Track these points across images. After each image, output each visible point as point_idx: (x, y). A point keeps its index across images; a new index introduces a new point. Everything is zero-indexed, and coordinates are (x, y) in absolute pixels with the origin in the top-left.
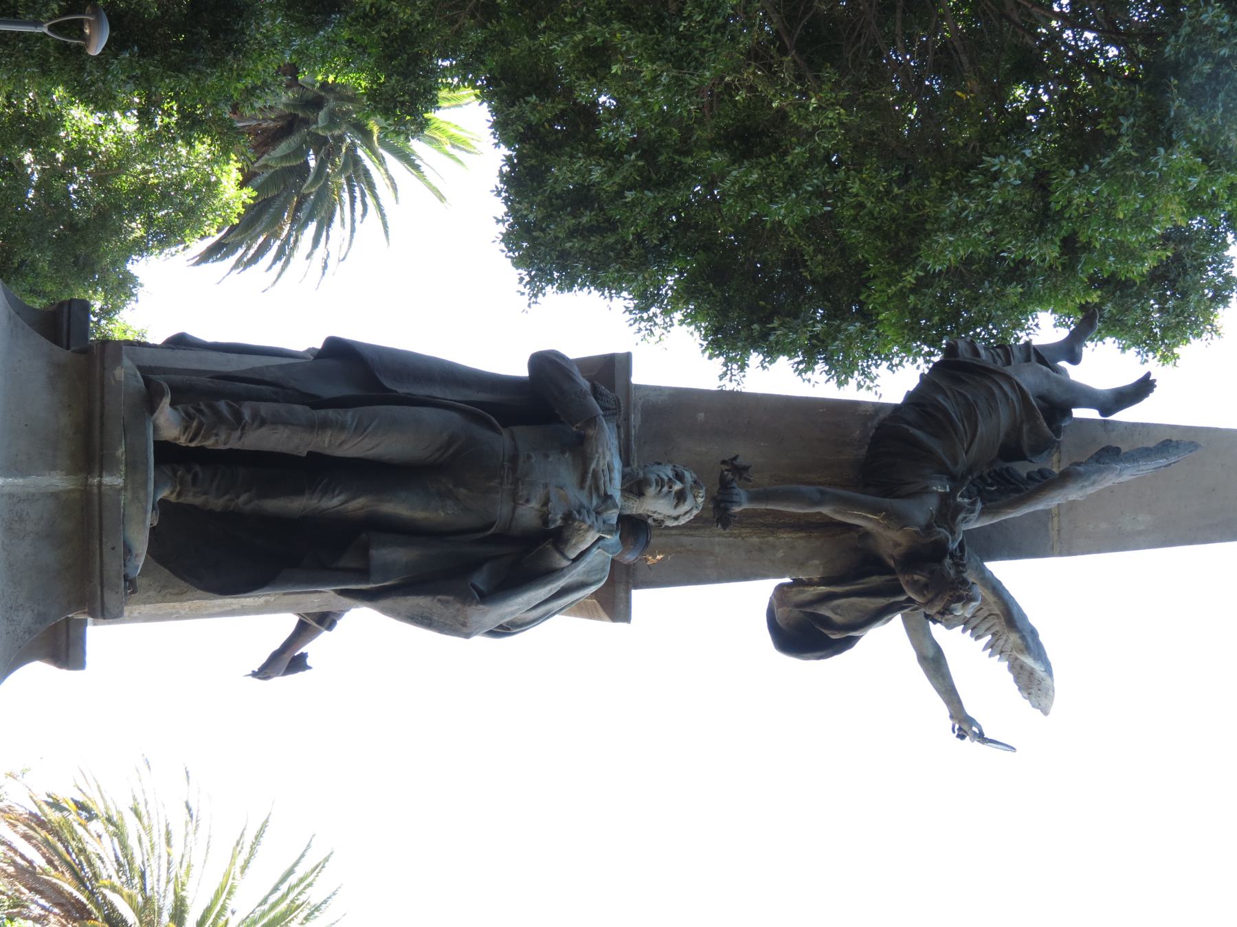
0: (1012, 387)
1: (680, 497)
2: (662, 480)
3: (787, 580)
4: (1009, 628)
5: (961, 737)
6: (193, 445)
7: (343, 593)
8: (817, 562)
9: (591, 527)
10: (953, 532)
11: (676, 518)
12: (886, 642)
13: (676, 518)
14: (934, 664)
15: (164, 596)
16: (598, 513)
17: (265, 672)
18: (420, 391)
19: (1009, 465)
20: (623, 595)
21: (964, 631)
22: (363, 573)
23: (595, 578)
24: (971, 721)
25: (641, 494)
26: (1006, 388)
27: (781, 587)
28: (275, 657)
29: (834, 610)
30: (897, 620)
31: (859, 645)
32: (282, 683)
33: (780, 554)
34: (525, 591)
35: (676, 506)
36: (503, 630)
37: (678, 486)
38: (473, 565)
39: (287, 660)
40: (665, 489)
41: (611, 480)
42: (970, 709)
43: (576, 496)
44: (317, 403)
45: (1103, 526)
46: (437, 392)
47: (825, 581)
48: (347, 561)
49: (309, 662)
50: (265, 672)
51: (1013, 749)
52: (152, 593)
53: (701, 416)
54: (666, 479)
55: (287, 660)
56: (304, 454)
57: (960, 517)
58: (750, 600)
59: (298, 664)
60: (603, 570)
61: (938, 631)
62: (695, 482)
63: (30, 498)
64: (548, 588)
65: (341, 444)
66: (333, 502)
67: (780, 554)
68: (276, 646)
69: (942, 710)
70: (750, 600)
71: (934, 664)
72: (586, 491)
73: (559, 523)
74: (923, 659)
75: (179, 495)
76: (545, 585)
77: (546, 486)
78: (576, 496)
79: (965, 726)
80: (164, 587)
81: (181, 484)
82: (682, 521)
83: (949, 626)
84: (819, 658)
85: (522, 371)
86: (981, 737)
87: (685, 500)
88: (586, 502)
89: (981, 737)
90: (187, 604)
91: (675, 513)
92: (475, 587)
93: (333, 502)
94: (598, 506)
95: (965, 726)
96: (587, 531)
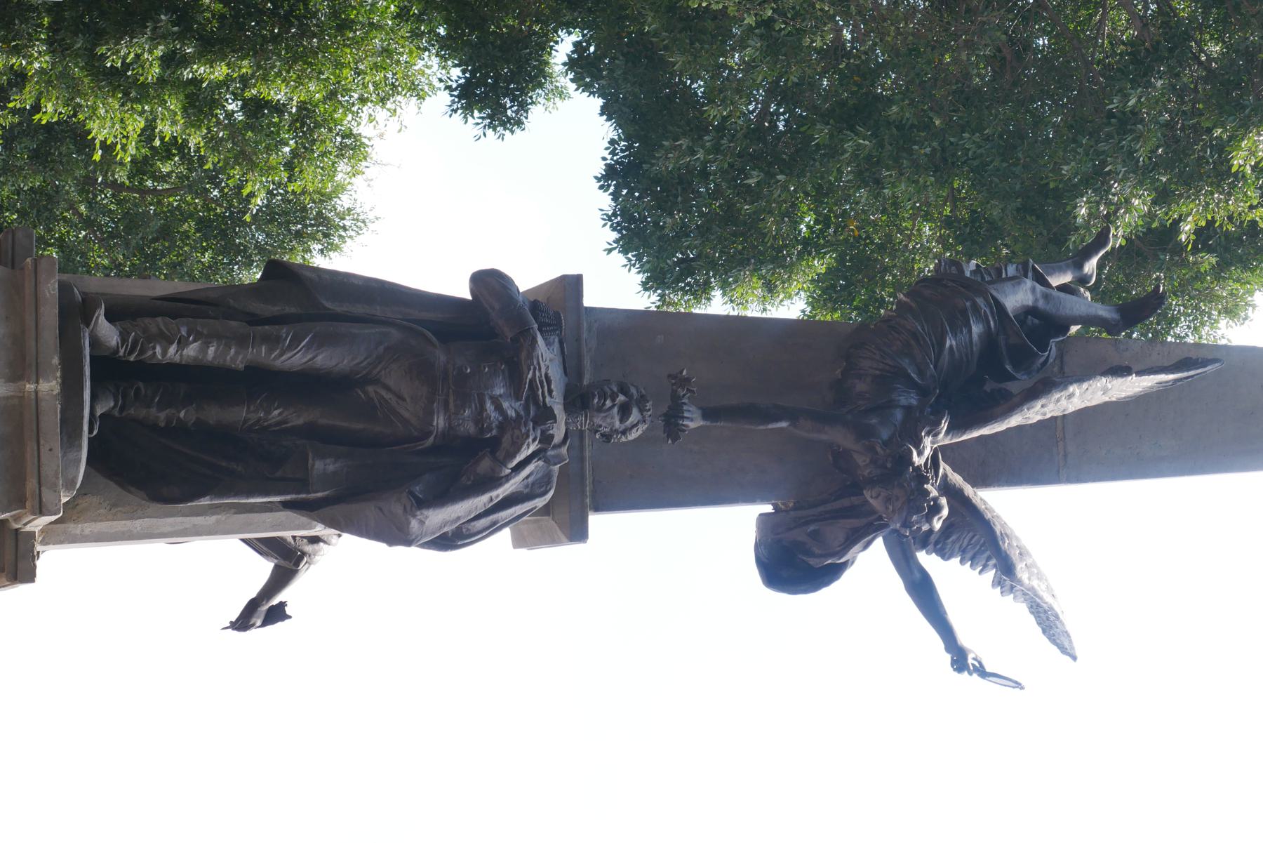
3: (768, 508)
4: (979, 539)
6: (132, 358)
7: (287, 505)
14: (923, 591)
17: (242, 623)
18: (359, 310)
19: (1003, 385)
21: (962, 562)
22: (303, 484)
23: (539, 491)
27: (763, 517)
28: (252, 606)
31: (848, 575)
32: (259, 635)
36: (448, 541)
37: (621, 398)
39: (262, 611)
41: (550, 392)
42: (963, 639)
43: (511, 408)
44: (254, 320)
46: (378, 311)
49: (288, 610)
50: (242, 623)
51: (1018, 685)
52: (102, 511)
55: (262, 611)
56: (241, 366)
58: (730, 531)
59: (277, 614)
61: (927, 560)
65: (275, 359)
68: (253, 594)
69: (937, 642)
70: (730, 531)
71: (923, 591)
73: (494, 432)
75: (122, 409)
78: (511, 408)
79: (960, 659)
80: (114, 505)
82: (633, 435)
83: (945, 556)
85: (463, 291)
86: (982, 672)
89: (982, 672)
90: (138, 525)
92: (411, 493)
95: (960, 659)
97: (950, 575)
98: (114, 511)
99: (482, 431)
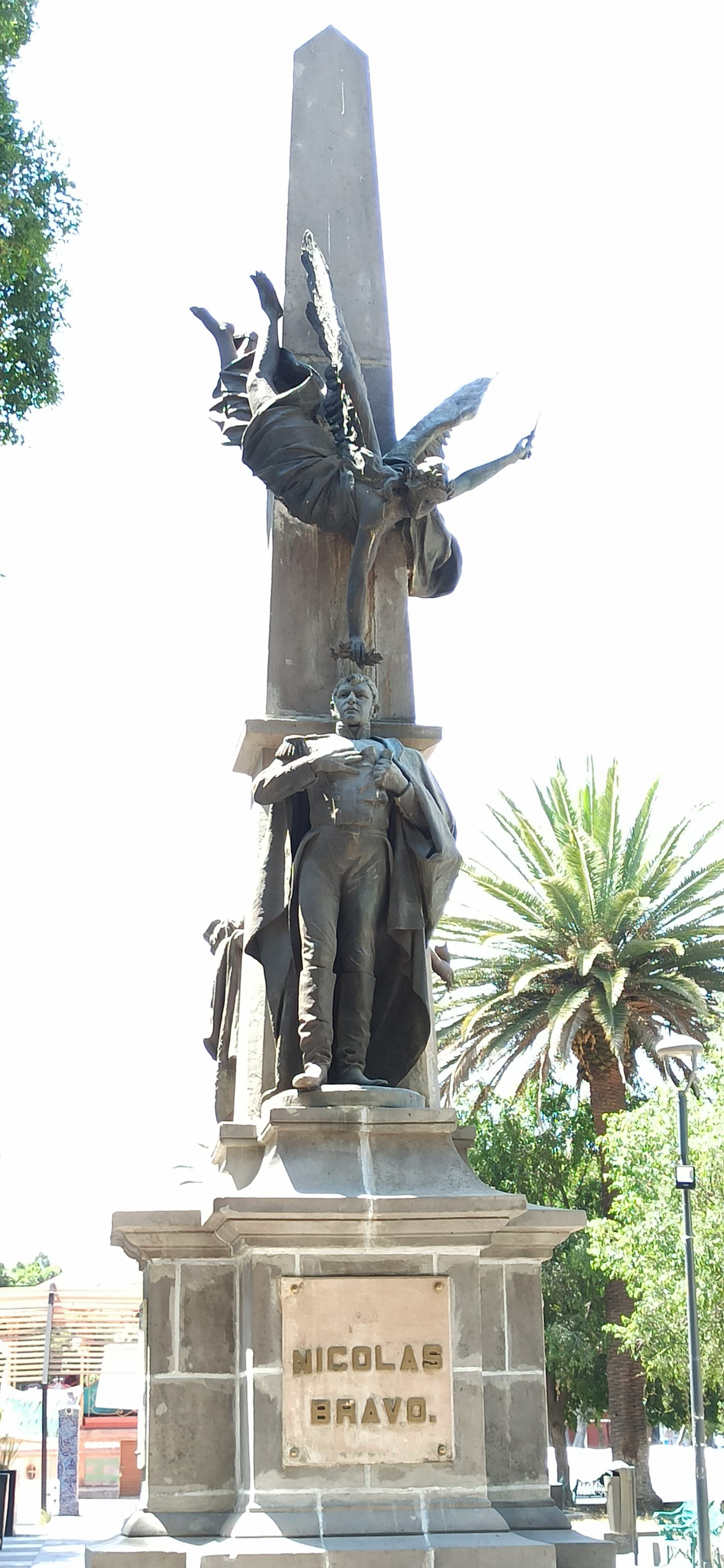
0: (273, 413)
1: (360, 695)
2: (348, 709)
5: (530, 454)
8: (396, 572)
9: (388, 769)
10: (388, 476)
11: (374, 697)
12: (455, 514)
13: (374, 697)
14: (473, 477)
15: (422, 1069)
16: (375, 763)
20: (423, 732)
21: (446, 444)
22: (414, 934)
23: (418, 760)
24: (518, 449)
25: (358, 725)
26: (272, 419)
29: (431, 559)
30: (443, 508)
33: (390, 602)
34: (431, 818)
35: (367, 698)
37: (352, 696)
38: (411, 855)
40: (355, 706)
42: (510, 450)
43: (363, 779)
45: (367, 318)
47: (410, 566)
48: (406, 945)
53: (288, 662)
54: (347, 705)
57: (375, 469)
60: (412, 754)
62: (348, 681)
63: (376, 1170)
64: (428, 800)
66: (366, 952)
67: (390, 602)
71: (473, 477)
72: (360, 770)
73: (385, 793)
74: (471, 486)
76: (426, 801)
77: (358, 801)
78: (363, 779)
79: (521, 452)
81: (353, 1062)
84: (461, 563)
87: (363, 691)
88: (369, 771)
89: (530, 438)
91: (371, 697)
93: (366, 952)
94: (371, 762)
95: (521, 452)
96: (391, 773)
97: (457, 455)
98: (419, 1070)
99: (383, 802)
